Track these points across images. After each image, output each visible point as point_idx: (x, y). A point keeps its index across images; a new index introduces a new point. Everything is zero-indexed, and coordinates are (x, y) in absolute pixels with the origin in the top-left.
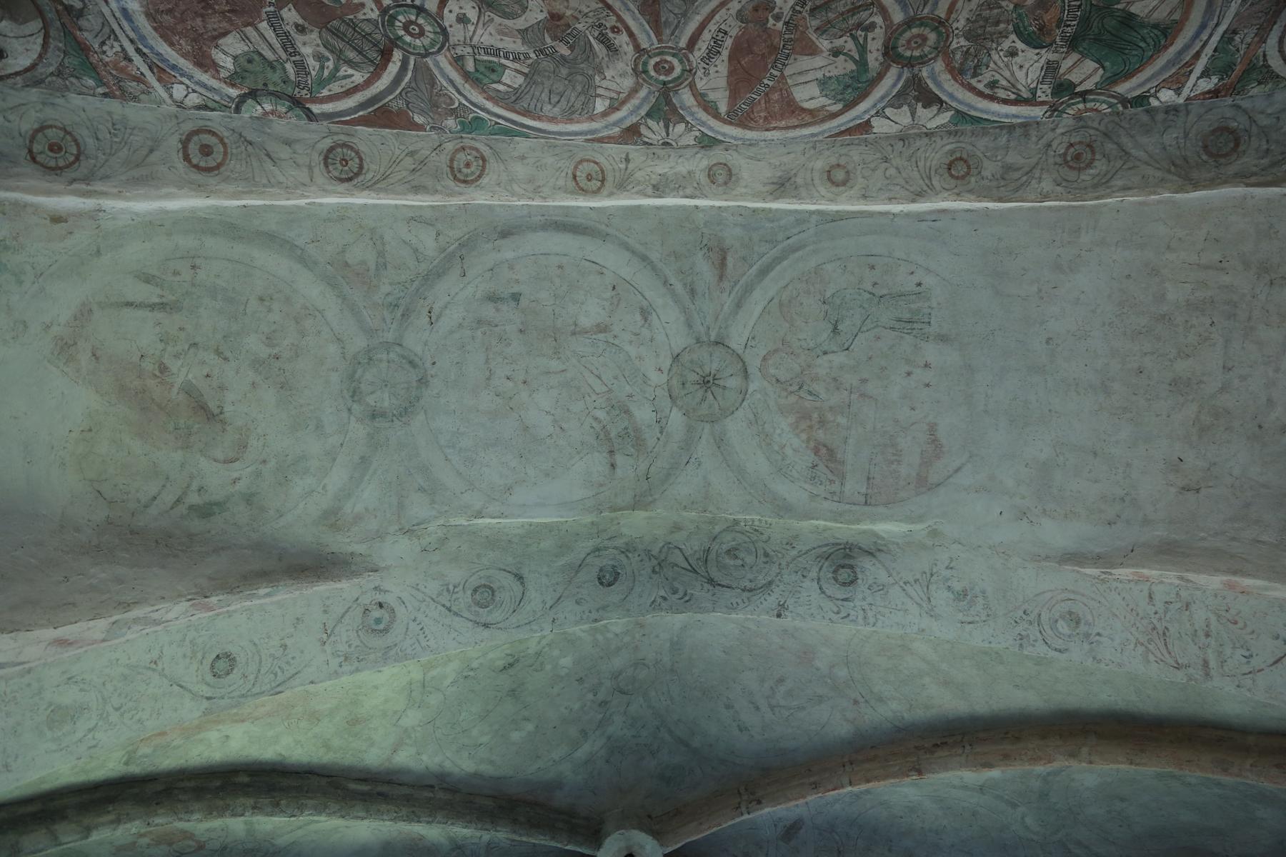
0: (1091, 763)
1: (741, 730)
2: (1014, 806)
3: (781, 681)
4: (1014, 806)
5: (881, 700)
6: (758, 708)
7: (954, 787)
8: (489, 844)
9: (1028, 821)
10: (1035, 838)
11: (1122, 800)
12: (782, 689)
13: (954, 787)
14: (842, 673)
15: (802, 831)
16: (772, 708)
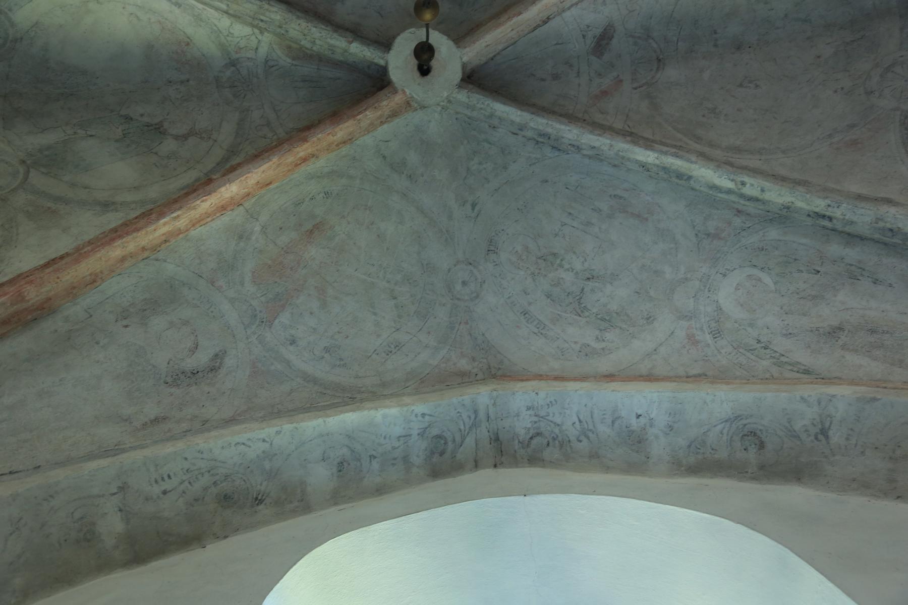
8: (266, 61)
15: (614, 41)
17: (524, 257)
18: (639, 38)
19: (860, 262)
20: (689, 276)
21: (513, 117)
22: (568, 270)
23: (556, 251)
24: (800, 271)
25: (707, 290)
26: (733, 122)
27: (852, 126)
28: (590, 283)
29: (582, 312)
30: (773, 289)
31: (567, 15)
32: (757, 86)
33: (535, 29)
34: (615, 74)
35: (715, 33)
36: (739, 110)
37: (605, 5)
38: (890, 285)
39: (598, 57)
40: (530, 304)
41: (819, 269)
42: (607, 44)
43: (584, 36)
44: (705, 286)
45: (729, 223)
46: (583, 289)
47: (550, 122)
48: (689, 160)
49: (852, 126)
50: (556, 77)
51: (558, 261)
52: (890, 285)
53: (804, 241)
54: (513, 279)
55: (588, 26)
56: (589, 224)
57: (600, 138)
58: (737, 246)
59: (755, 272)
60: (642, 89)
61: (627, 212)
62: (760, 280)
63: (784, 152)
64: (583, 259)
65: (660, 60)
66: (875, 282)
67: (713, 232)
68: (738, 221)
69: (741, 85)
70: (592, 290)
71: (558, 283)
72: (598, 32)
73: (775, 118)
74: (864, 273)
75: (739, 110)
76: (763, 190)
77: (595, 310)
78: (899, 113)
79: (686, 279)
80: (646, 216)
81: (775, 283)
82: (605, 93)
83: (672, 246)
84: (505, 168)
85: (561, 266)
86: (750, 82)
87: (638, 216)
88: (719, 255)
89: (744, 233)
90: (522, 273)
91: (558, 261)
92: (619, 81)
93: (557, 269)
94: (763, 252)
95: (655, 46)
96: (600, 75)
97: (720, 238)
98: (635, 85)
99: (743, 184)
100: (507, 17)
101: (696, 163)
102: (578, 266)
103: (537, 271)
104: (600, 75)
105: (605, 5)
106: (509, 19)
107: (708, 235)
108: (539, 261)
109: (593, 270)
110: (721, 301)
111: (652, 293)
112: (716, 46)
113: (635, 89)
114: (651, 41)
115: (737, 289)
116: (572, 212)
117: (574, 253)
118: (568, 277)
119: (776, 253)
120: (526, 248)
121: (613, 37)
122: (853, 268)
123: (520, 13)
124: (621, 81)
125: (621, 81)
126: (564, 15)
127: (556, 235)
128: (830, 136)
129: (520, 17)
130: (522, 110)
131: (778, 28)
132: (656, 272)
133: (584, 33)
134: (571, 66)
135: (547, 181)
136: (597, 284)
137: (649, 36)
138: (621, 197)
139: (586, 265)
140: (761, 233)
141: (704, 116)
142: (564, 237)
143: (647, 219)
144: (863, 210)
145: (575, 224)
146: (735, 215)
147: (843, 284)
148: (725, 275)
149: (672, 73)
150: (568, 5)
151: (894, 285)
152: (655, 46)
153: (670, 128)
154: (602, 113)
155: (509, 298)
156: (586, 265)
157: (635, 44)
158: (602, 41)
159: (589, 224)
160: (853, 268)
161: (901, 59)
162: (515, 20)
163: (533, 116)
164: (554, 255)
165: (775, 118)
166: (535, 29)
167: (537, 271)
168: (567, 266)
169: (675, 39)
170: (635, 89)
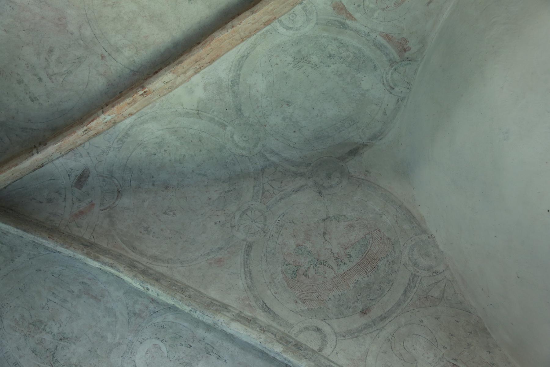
0: (233, 27)
1: (32, 101)
2: (224, 126)
3: (51, 51)
4: (224, 126)
5: (118, 50)
6: (40, 80)
7: (180, 115)
9: (236, 138)
10: (244, 153)
11: (288, 104)
12: (54, 58)
13: (180, 115)
14: (87, 32)
15: (90, 179)
16: (50, 77)
17: (20, 323)
18: (106, 177)
19: (212, 342)
20: (121, 341)
21: (12, 232)
22: (49, 333)
23: (41, 319)
24: (182, 345)
25: (130, 353)
26: (157, 238)
27: (220, 249)
28: (62, 343)
29: (54, 363)
30: (166, 355)
31: (57, 162)
32: (174, 214)
33: (34, 170)
34: (90, 200)
35: (153, 177)
36: (162, 230)
37: (82, 157)
38: (225, 361)
39: (79, 189)
40: (20, 357)
41: (191, 345)
42: (85, 180)
43: (69, 175)
44: (129, 350)
45: (147, 308)
46: (56, 347)
47: (36, 237)
48: (118, 270)
49: (220, 249)
50: (50, 201)
51: (43, 327)
52: (225, 361)
53: (186, 324)
54: (11, 339)
55: (72, 169)
56: (65, 301)
57: (68, 250)
58: (150, 324)
59: (158, 342)
60: (106, 211)
61: (89, 294)
62: (160, 348)
63: (181, 263)
64: (58, 326)
65: (119, 192)
66: (218, 358)
67: (137, 312)
68: (152, 307)
69: (165, 213)
70: (63, 348)
71: (41, 342)
72: (79, 173)
73: (181, 238)
74: (214, 351)
75: (162, 230)
76: (158, 295)
77: (62, 363)
78: (245, 243)
79: (119, 343)
80: (100, 298)
81: (168, 352)
82: (81, 213)
83: (114, 319)
84: (13, 260)
85: (44, 330)
86: (171, 211)
87: (95, 298)
88: (139, 328)
89: (154, 315)
90: (18, 334)
91: (43, 327)
92: (92, 205)
93: (41, 332)
94: (163, 329)
95: (117, 182)
96: (80, 200)
97: (141, 317)
98: (102, 208)
99: (148, 289)
100: (8, 167)
101: (122, 272)
102: (55, 330)
103: (28, 333)
104: (80, 200)
105: (82, 157)
106: (9, 168)
107: (135, 314)
108: (30, 326)
109: (65, 333)
110: (136, 361)
111: (98, 352)
112: (153, 185)
113: (102, 210)
114: (114, 179)
115: (147, 353)
116: (55, 292)
117: (54, 320)
118: (48, 338)
119: (171, 331)
120: (22, 317)
121: (89, 176)
122: (208, 346)
123: (17, 165)
124: (93, 205)
125: (93, 205)
126: (54, 162)
127: (43, 308)
128: (208, 254)
129: (17, 167)
130: (17, 228)
131: (189, 178)
132: (102, 337)
133: (69, 173)
134: (60, 194)
135: (40, 270)
136: (66, 343)
137: (112, 176)
138: (86, 284)
139: (61, 329)
140: (164, 316)
141: (141, 232)
142: (48, 310)
143: (100, 301)
144: (207, 317)
145: (56, 301)
146: (151, 302)
147: (202, 357)
148: (141, 343)
149: (126, 201)
150: (56, 157)
151: (227, 361)
152: (117, 182)
153: (119, 240)
154: (78, 227)
155: (7, 353)
156: (61, 329)
157: (104, 181)
158: (82, 179)
159: (65, 301)
160: (208, 346)
161: (252, 206)
162: (13, 169)
163: (24, 233)
164: (41, 321)
165: (181, 238)
166: (34, 170)
167: (28, 333)
168: (48, 330)
169: (129, 179)
170: (102, 210)
